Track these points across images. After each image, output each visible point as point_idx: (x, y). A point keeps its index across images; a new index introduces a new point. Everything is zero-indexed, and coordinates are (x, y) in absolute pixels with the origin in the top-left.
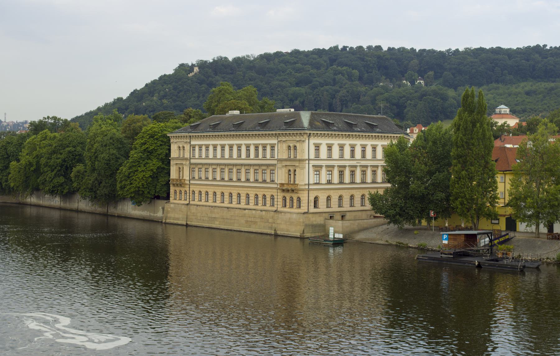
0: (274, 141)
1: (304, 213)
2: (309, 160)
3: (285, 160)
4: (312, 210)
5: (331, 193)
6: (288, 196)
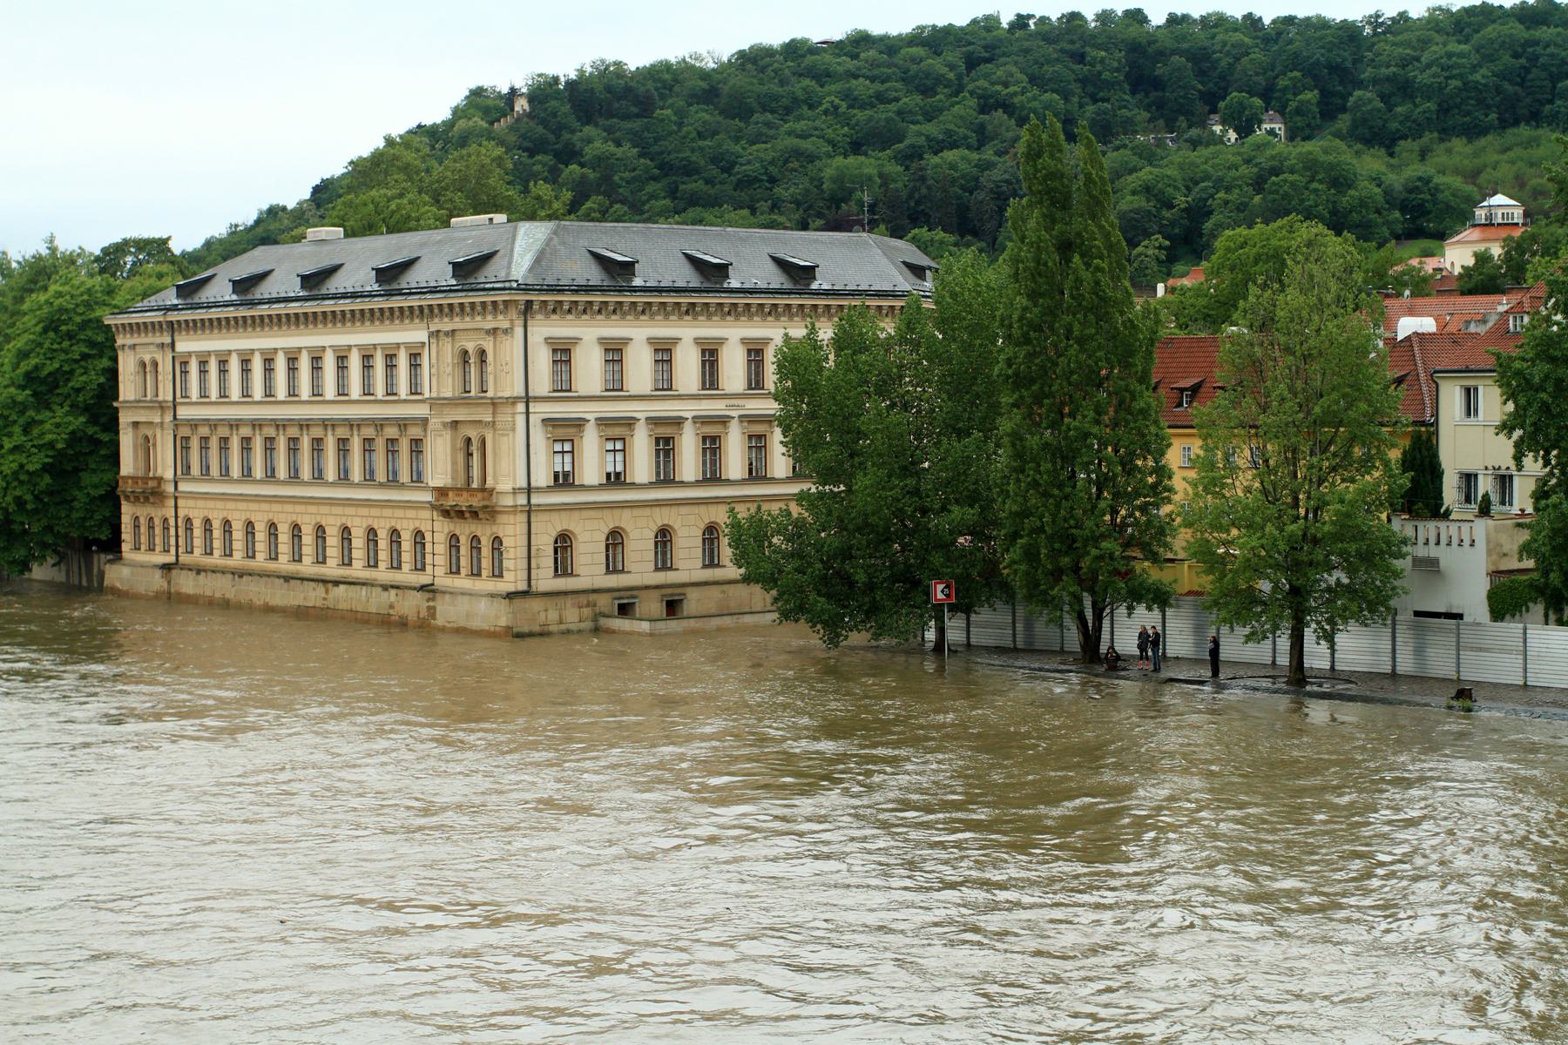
0: (415, 334)
1: (510, 596)
2: (528, 400)
3: (451, 402)
4: (545, 580)
5: (625, 520)
6: (464, 530)
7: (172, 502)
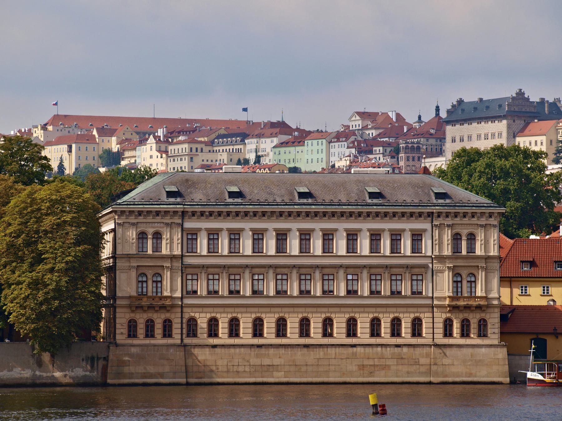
0: (427, 226)
7: (180, 310)
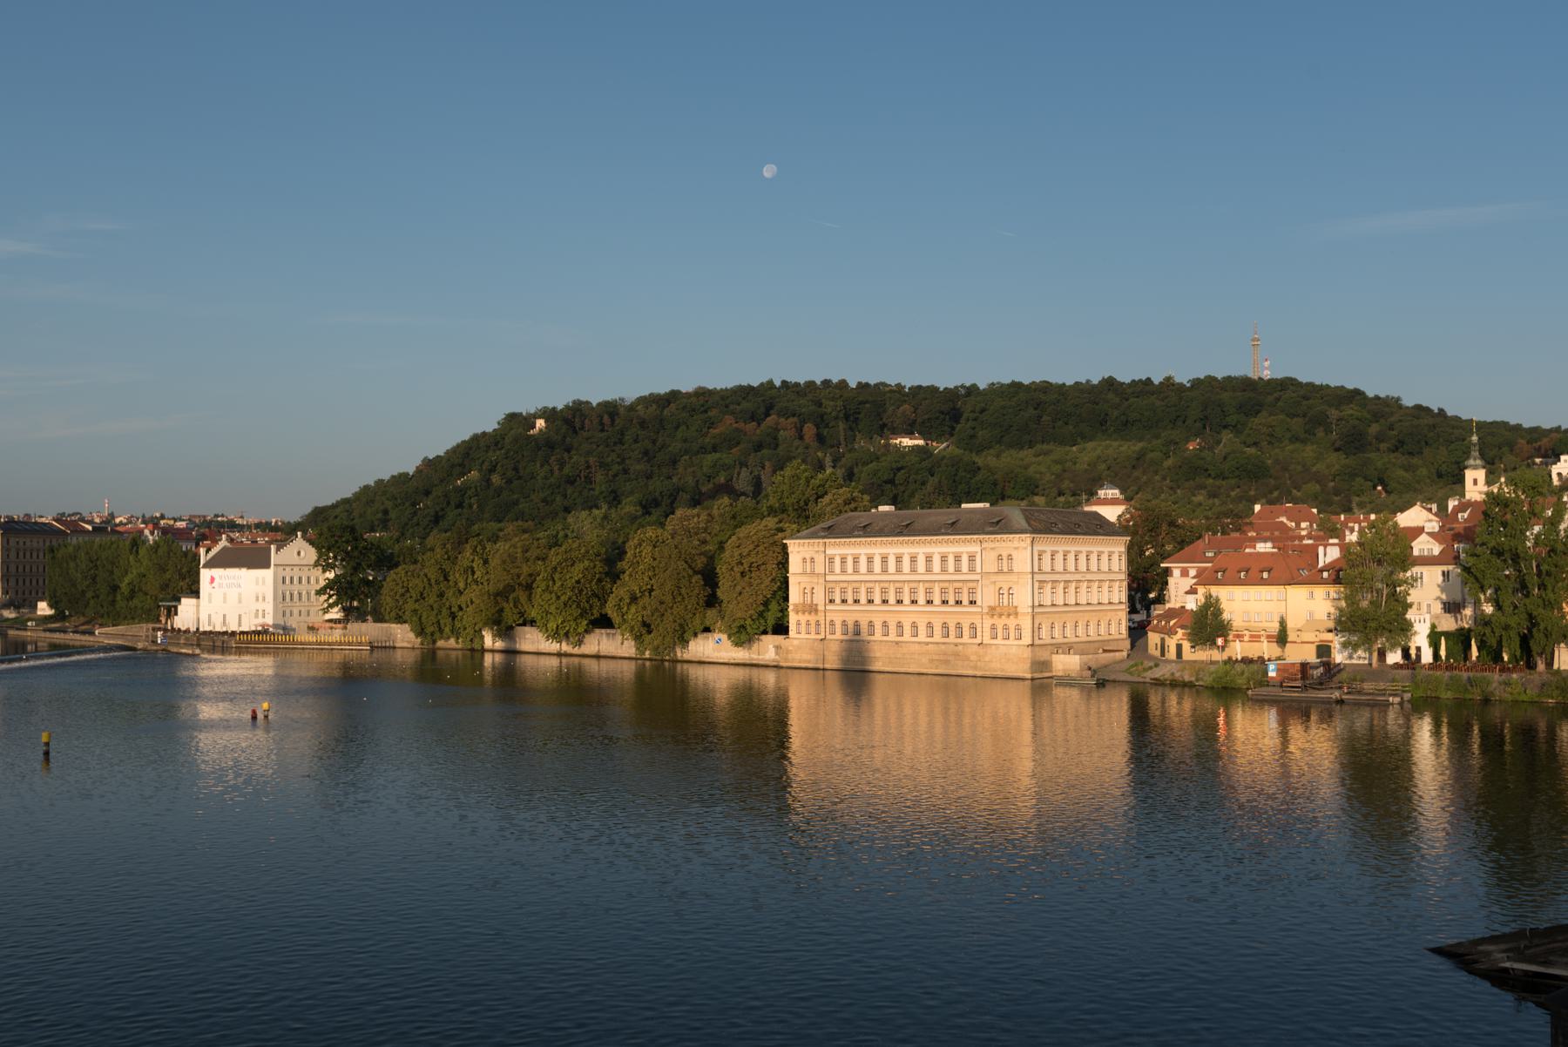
0: (975, 548)
6: (1000, 622)
